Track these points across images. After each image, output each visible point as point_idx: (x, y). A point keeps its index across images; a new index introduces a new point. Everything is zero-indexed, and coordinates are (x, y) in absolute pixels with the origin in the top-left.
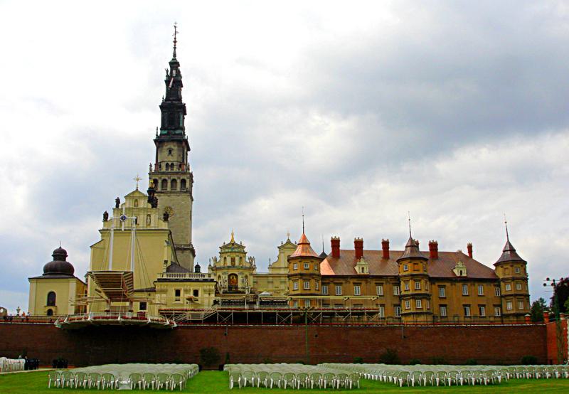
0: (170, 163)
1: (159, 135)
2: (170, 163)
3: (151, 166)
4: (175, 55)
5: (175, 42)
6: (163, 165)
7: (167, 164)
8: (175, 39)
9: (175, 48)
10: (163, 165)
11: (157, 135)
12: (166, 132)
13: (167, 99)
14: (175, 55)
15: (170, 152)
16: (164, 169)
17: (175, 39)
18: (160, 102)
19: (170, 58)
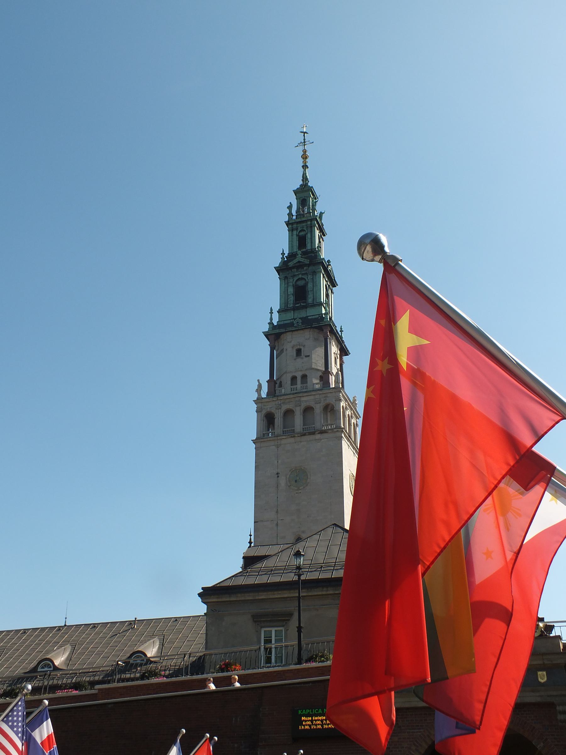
0: (299, 375)
1: (275, 324)
2: (299, 375)
3: (260, 386)
4: (305, 178)
5: (305, 157)
6: (287, 380)
7: (294, 379)
8: (305, 151)
9: (305, 167)
10: (287, 380)
11: (271, 323)
12: (290, 316)
13: (292, 256)
14: (305, 178)
15: (299, 352)
16: (287, 388)
17: (305, 151)
18: (277, 262)
19: (298, 183)
